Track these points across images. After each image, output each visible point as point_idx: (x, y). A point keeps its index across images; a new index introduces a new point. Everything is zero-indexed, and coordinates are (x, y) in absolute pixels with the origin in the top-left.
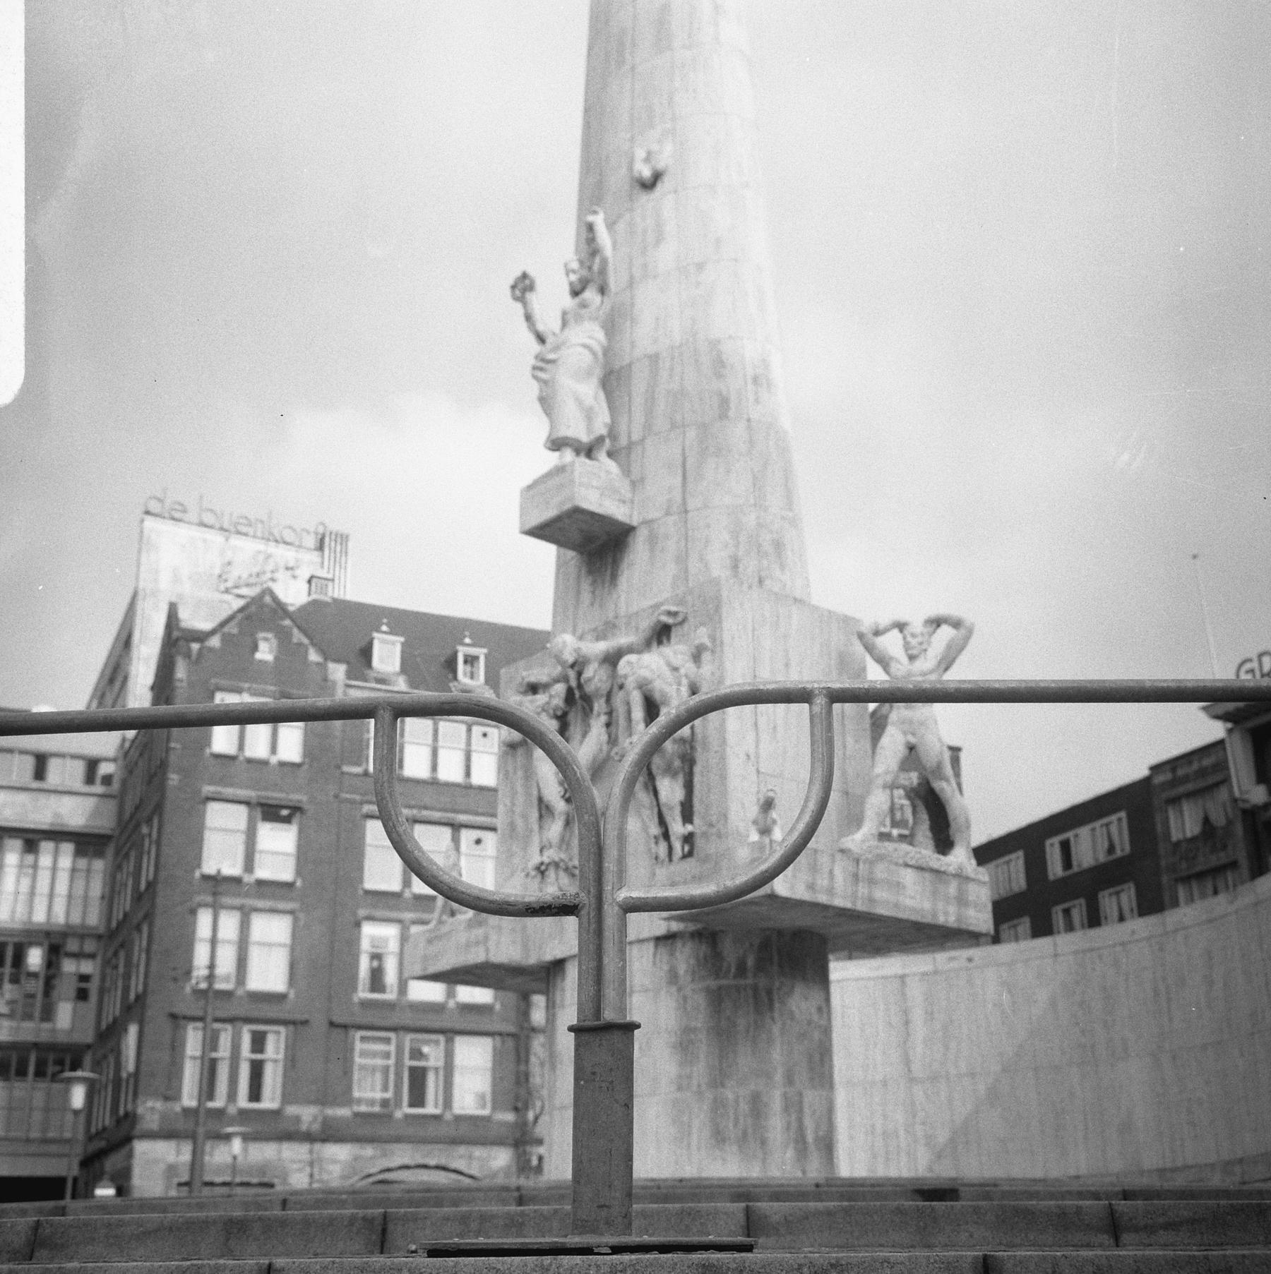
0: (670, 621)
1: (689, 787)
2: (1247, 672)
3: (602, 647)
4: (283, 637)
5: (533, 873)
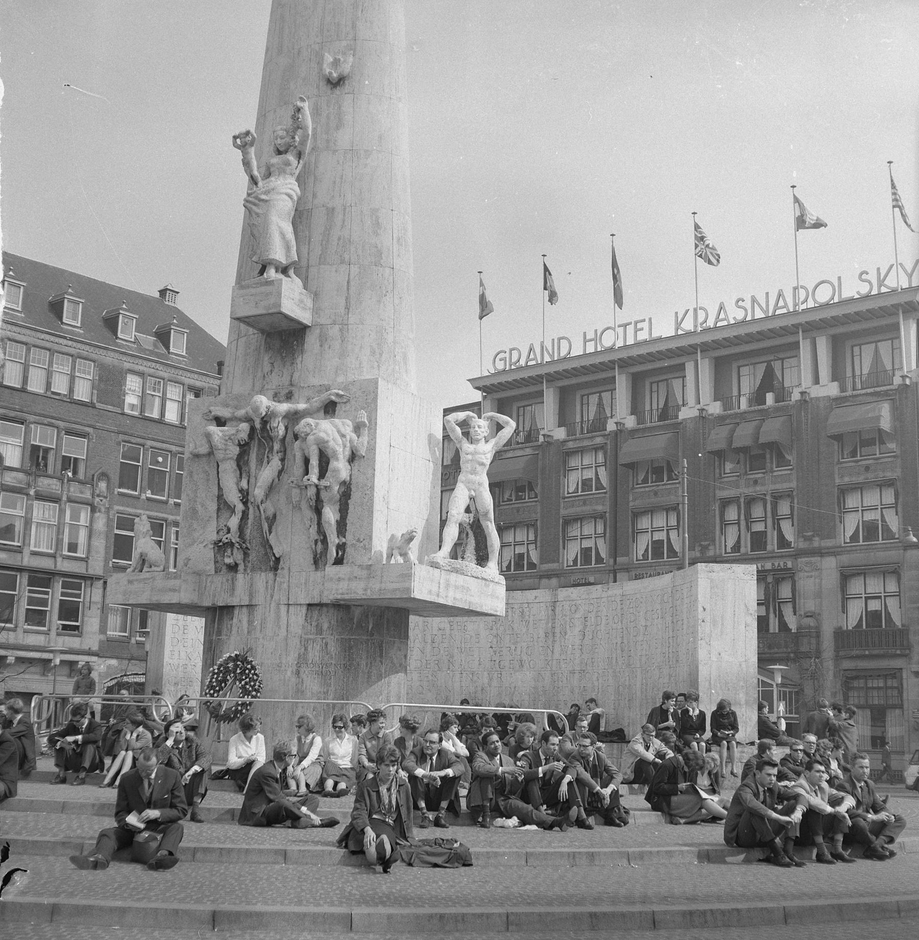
1: (344, 510)
3: (284, 407)
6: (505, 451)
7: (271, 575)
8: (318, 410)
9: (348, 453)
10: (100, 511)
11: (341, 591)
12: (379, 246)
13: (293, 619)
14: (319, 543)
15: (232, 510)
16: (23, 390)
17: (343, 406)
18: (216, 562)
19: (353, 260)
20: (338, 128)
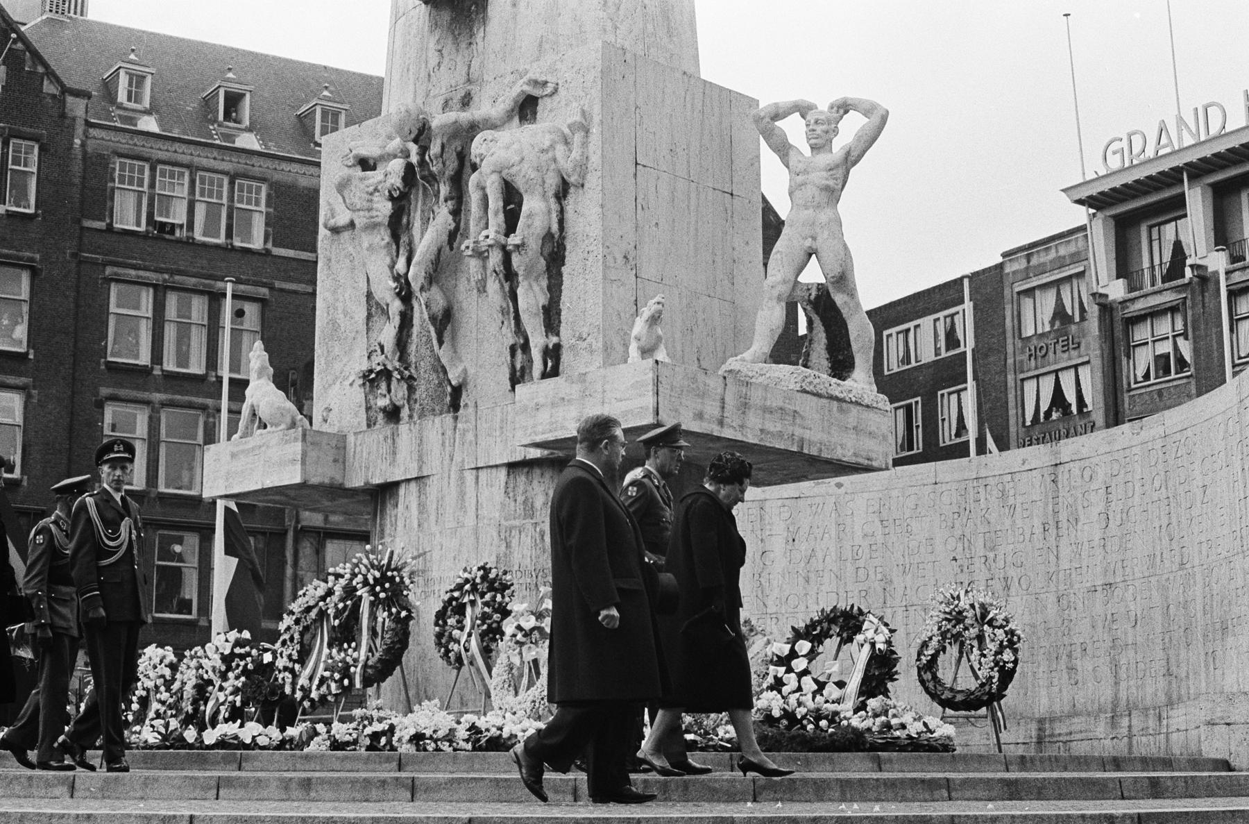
0: (536, 92)
1: (555, 288)
2: (1114, 153)
5: (361, 381)
6: (1133, 300)
7: (448, 418)
8: (509, 117)
9: (552, 182)
11: (540, 428)
13: (485, 493)
14: (519, 351)
15: (385, 312)
17: (548, 100)
18: (368, 409)
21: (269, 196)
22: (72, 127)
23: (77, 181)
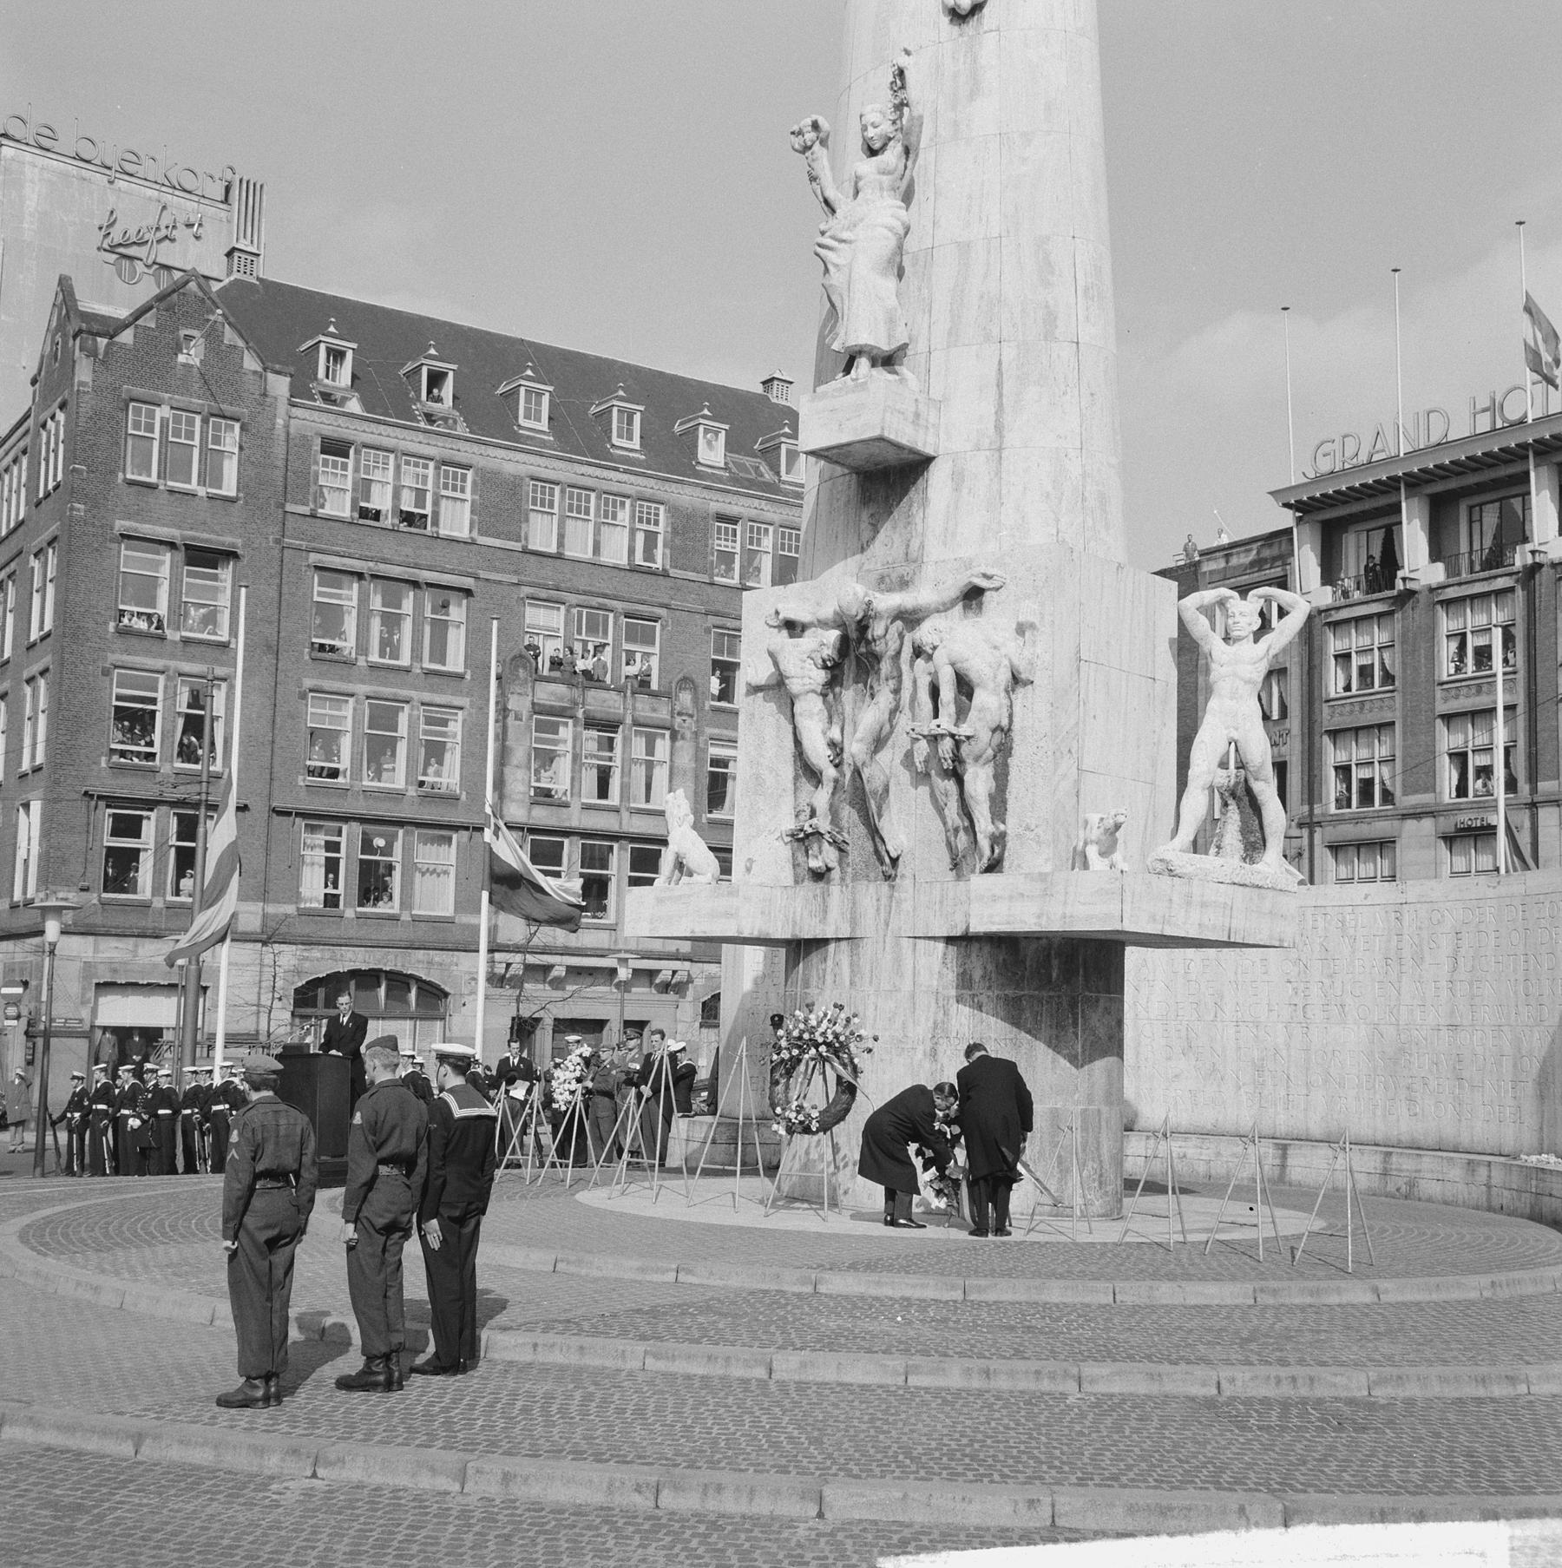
0: (983, 583)
1: (1001, 777)
4: (213, 337)
6: (1338, 609)
8: (953, 603)
9: (1004, 677)
10: (683, 738)
11: (997, 919)
12: (1051, 302)
16: (559, 557)
18: (795, 866)
19: (1005, 335)
20: (973, 95)
21: (474, 483)
22: (273, 406)
23: (280, 463)
